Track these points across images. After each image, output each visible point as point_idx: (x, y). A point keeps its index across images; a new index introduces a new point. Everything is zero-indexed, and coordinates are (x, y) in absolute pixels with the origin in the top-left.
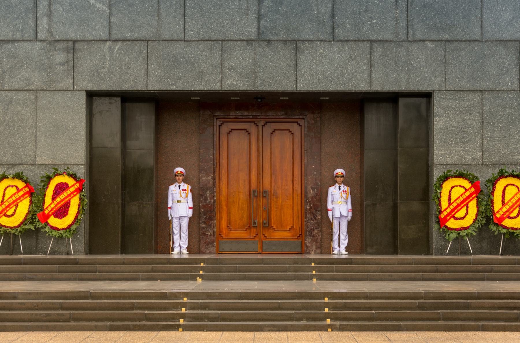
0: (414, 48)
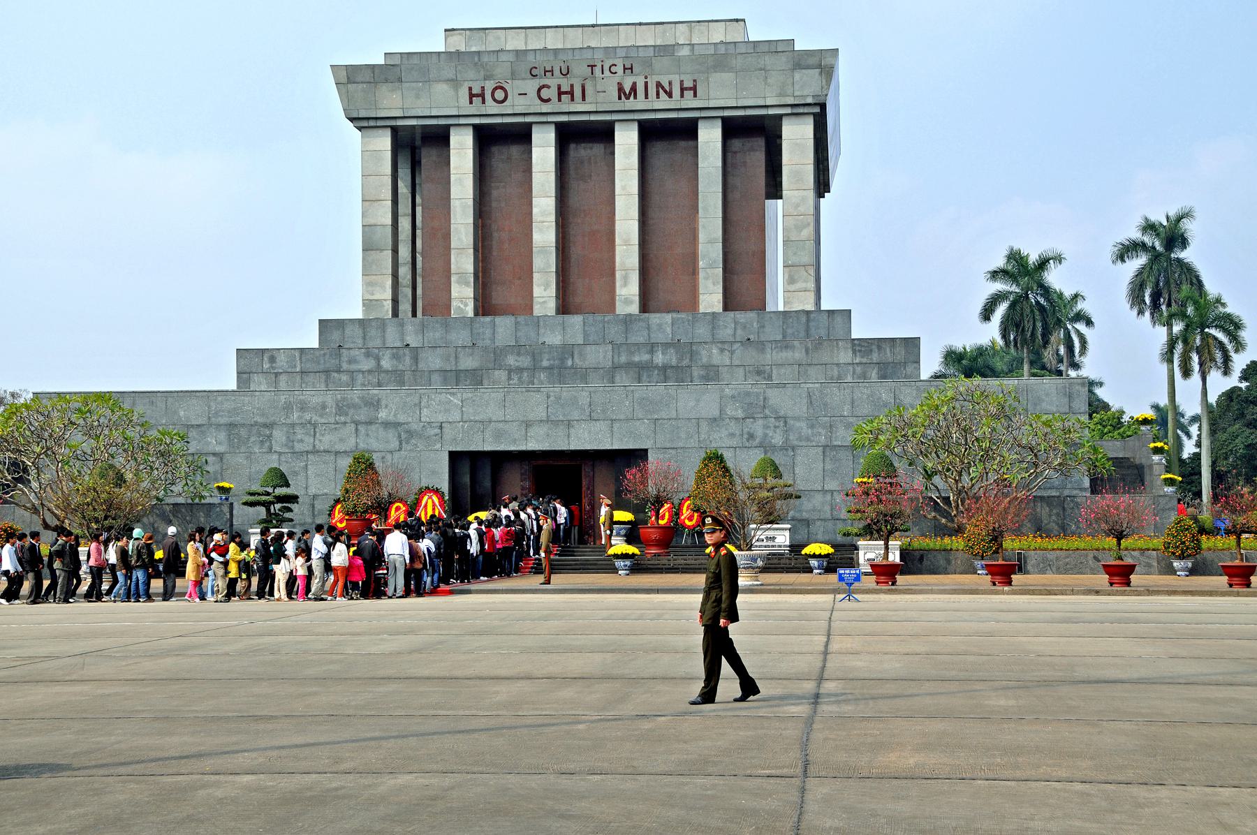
0: (638, 423)
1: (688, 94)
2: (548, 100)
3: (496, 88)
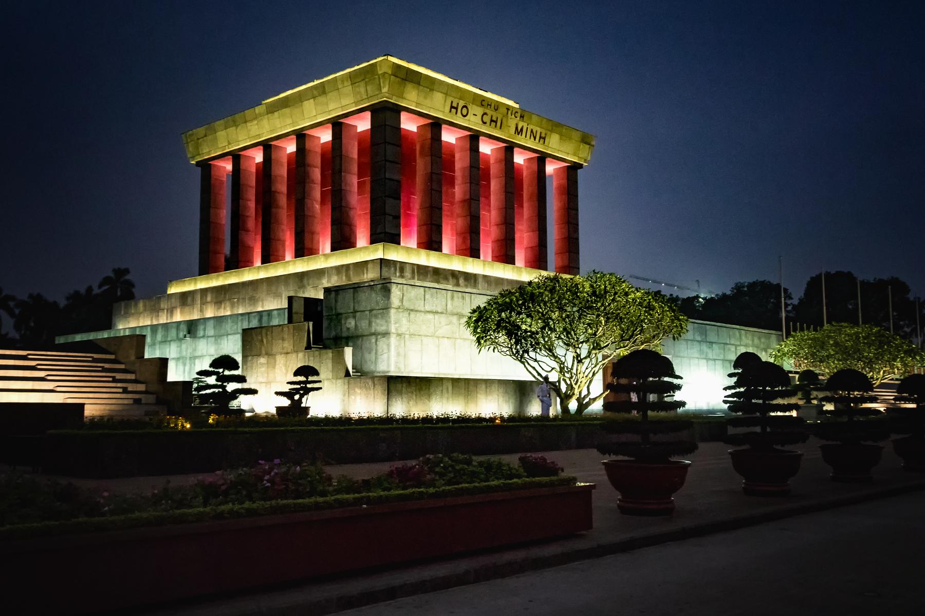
1: (542, 141)
2: (485, 123)
3: (464, 107)
